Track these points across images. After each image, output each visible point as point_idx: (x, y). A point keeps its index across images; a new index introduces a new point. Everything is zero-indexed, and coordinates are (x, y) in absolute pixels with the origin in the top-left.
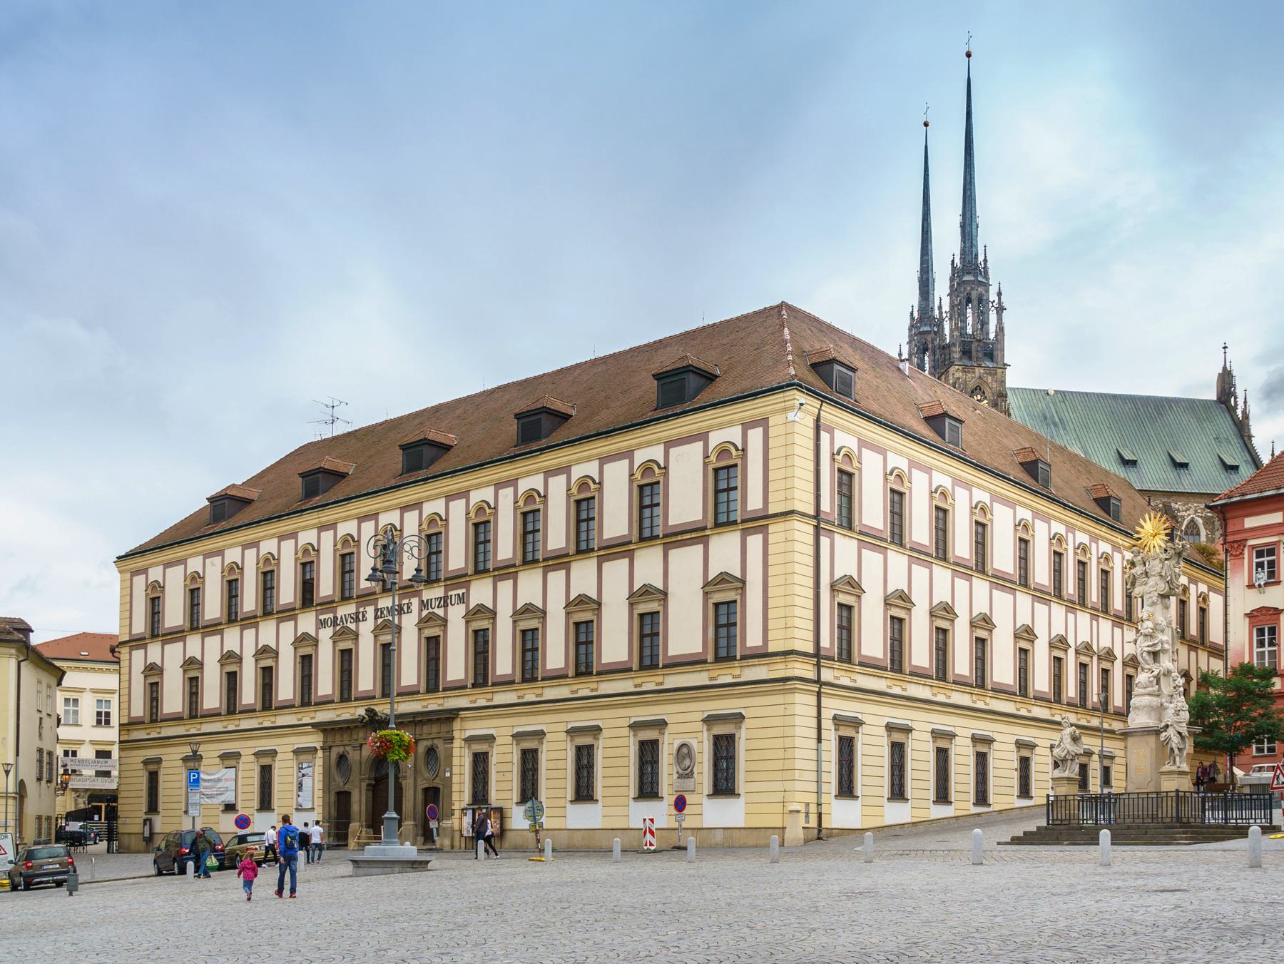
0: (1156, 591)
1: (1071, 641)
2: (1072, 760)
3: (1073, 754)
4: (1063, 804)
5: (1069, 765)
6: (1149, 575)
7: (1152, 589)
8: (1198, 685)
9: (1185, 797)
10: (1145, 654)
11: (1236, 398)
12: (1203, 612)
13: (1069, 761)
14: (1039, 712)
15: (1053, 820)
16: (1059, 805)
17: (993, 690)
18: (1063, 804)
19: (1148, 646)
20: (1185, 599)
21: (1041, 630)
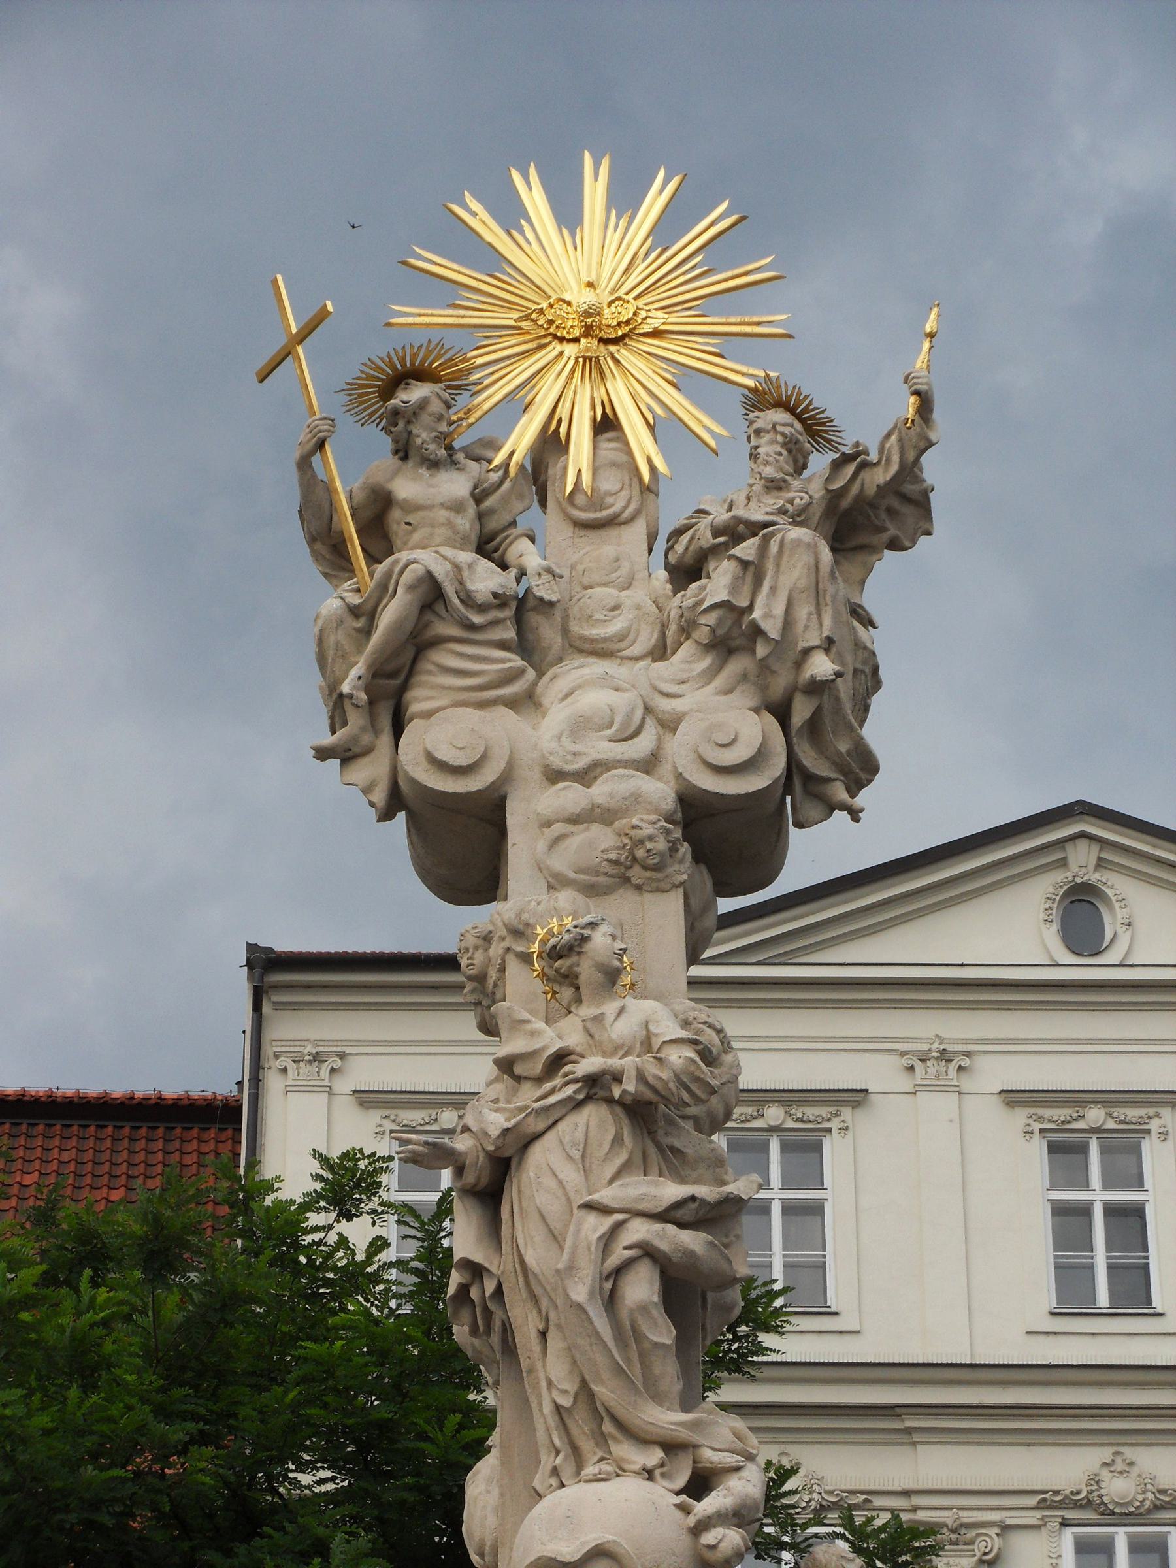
0: (648, 765)
6: (547, 632)
7: (600, 747)
19: (663, 1216)
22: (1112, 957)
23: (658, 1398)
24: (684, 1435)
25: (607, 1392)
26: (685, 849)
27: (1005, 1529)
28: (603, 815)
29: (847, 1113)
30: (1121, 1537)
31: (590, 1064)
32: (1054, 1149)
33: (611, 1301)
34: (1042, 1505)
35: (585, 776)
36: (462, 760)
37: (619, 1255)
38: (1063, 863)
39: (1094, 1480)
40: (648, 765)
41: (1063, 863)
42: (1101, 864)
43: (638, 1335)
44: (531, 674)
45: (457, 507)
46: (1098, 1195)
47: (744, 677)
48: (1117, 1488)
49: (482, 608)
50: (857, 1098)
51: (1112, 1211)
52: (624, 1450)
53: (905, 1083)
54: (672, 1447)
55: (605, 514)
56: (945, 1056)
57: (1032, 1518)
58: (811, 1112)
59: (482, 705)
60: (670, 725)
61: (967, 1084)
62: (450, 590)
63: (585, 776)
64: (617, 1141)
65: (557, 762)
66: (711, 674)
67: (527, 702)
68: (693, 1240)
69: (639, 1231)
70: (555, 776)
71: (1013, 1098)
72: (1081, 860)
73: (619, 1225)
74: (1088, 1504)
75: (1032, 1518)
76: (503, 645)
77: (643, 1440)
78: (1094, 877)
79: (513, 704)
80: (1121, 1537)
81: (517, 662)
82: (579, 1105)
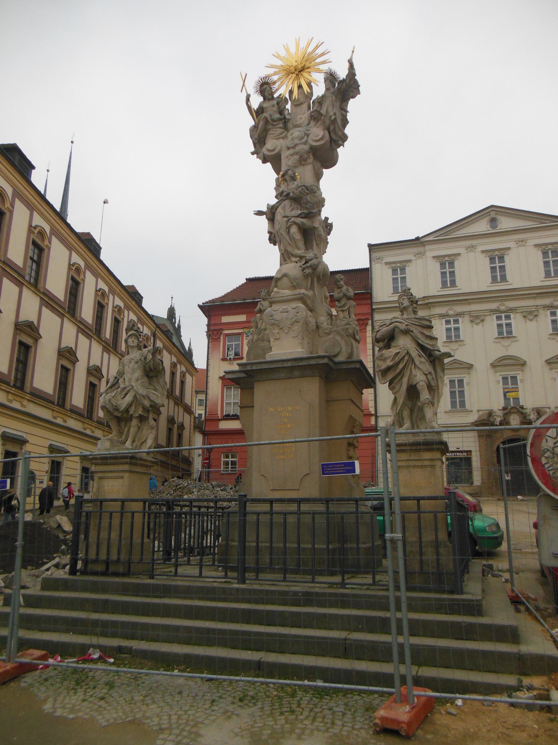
0: (305, 143)
1: (104, 372)
2: (142, 419)
3: (147, 403)
4: (116, 521)
5: (133, 430)
6: (290, 125)
7: (297, 141)
8: (178, 428)
9: (419, 511)
10: (294, 230)
11: (175, 319)
12: (183, 383)
13: (135, 422)
14: (72, 423)
15: (86, 562)
16: (105, 522)
17: (32, 394)
18: (116, 521)
20: (175, 371)
21: (81, 354)
22: (498, 228)
23: (299, 249)
24: (303, 255)
25: (289, 249)
26: (311, 157)
27: (485, 315)
28: (297, 153)
30: (503, 315)
32: (490, 259)
33: (289, 232)
34: (491, 311)
35: (294, 147)
36: (272, 148)
37: (289, 224)
38: (490, 215)
39: (498, 307)
40: (305, 143)
41: (490, 215)
43: (294, 238)
44: (286, 132)
45: (273, 106)
47: (321, 124)
48: (502, 308)
49: (275, 121)
50: (459, 254)
52: (294, 259)
53: (466, 252)
54: (301, 257)
55: (299, 102)
56: (472, 247)
58: (452, 257)
59: (277, 139)
60: (308, 136)
61: (476, 250)
62: (269, 119)
63: (294, 147)
64: (291, 205)
65: (289, 146)
66: (315, 125)
67: (285, 137)
68: (304, 221)
69: (293, 219)
70: (288, 148)
71: (483, 252)
72: (493, 214)
73: (289, 219)
74: (497, 311)
76: (280, 128)
77: (296, 256)
78: (495, 216)
79: (283, 138)
80: (503, 315)
81: (282, 130)
82: (285, 200)
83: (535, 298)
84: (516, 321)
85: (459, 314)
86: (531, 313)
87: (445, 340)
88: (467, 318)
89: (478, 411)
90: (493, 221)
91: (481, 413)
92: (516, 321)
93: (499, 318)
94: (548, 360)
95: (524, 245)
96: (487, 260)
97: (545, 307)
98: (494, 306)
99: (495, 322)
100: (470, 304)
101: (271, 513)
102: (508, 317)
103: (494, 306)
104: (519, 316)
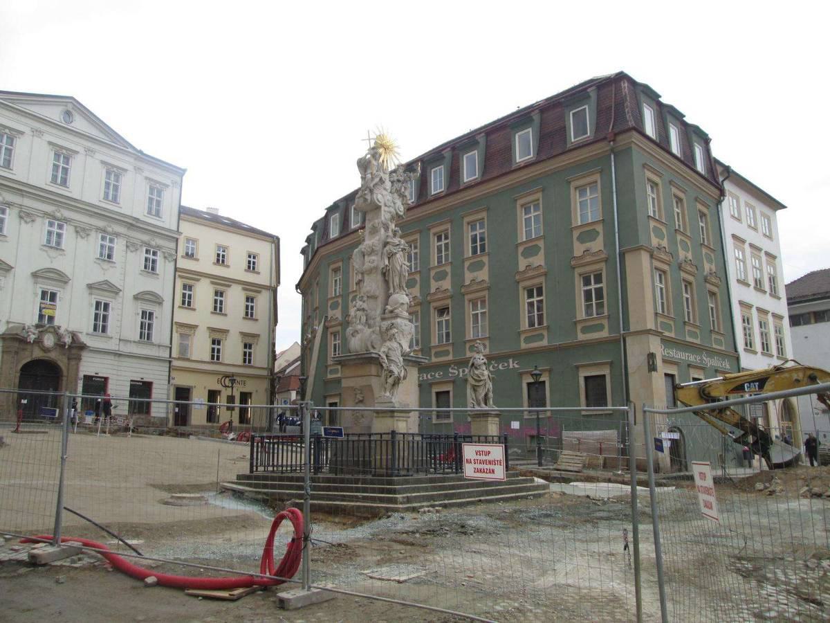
29: (20, 136)
30: (56, 222)
31: (402, 247)
32: (55, 154)
38: (66, 106)
42: (73, 108)
46: (62, 165)
48: (58, 215)
51: (63, 168)
53: (32, 133)
56: (40, 132)
57: (41, 215)
58: (14, 133)
70: (386, 206)
72: (70, 107)
74: (52, 216)
75: (41, 215)
83: (91, 216)
84: (68, 233)
85: (7, 204)
86: (84, 230)
87: (45, 244)
88: (15, 211)
89: (8, 322)
90: (68, 114)
91: (11, 325)
92: (68, 233)
93: (51, 224)
94: (91, 284)
95: (92, 157)
96: (52, 155)
97: (98, 229)
98: (49, 208)
99: (47, 228)
100: (23, 196)
101: (348, 441)
102: (60, 227)
103: (49, 208)
104: (71, 229)
